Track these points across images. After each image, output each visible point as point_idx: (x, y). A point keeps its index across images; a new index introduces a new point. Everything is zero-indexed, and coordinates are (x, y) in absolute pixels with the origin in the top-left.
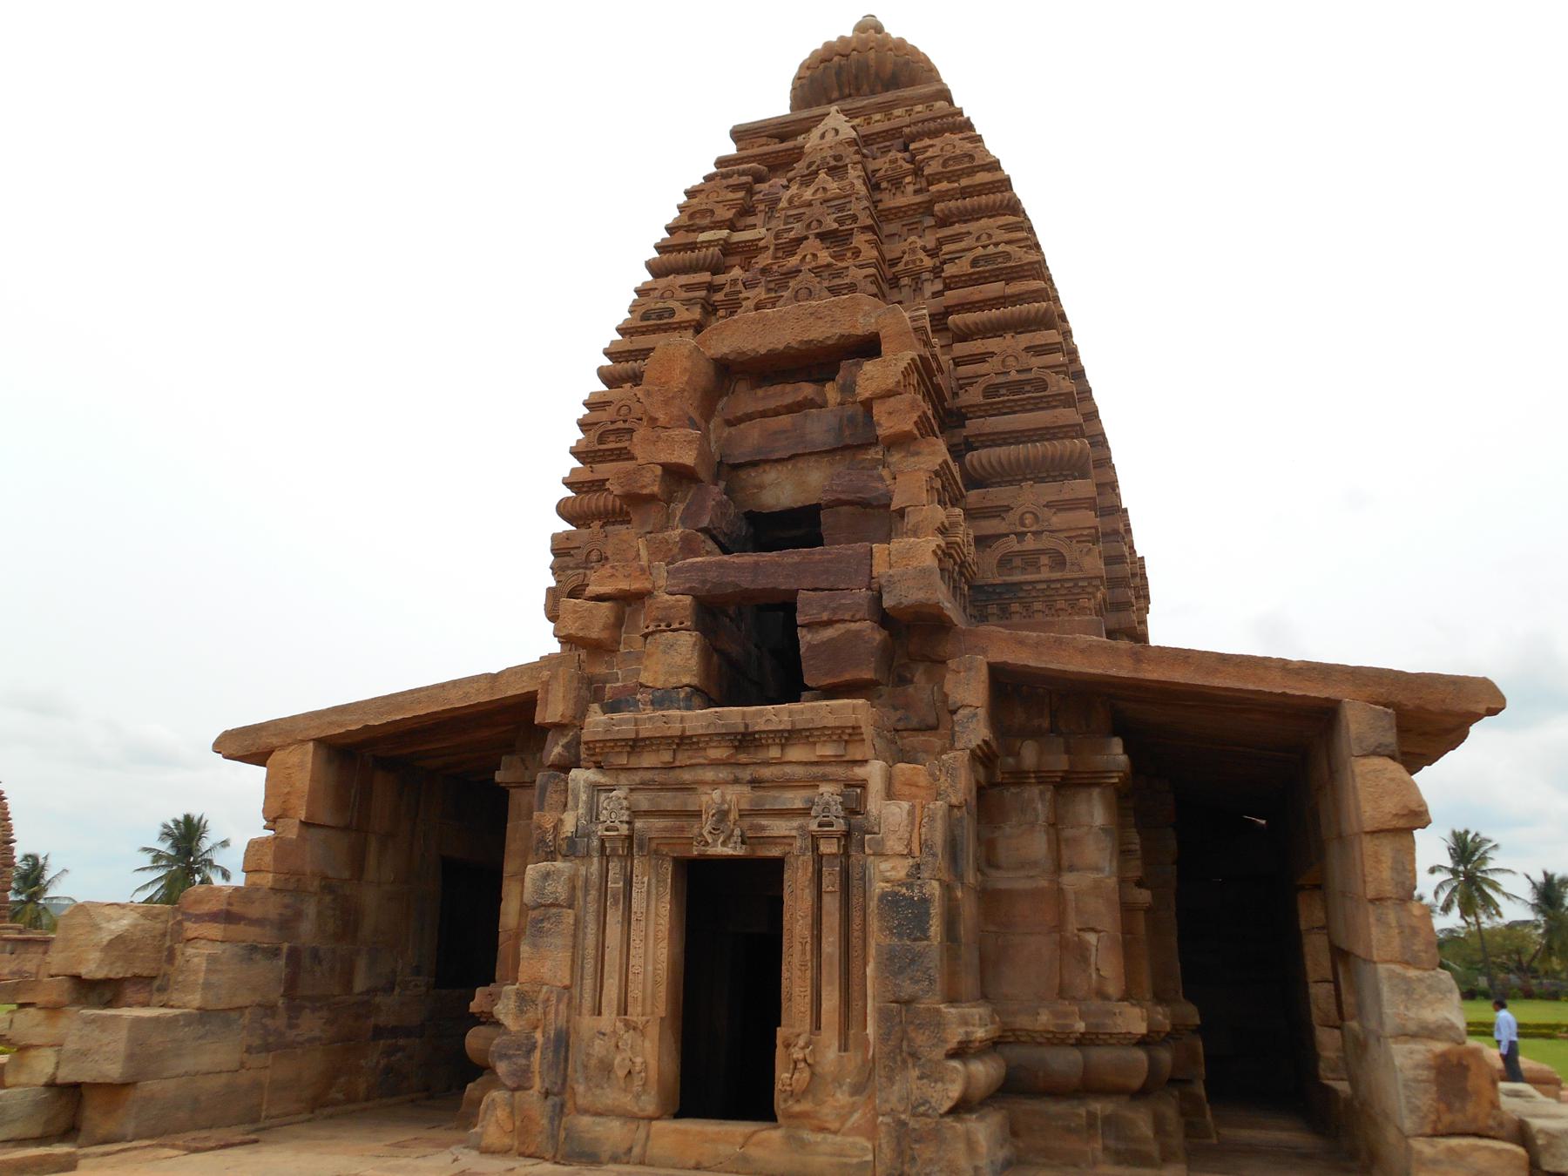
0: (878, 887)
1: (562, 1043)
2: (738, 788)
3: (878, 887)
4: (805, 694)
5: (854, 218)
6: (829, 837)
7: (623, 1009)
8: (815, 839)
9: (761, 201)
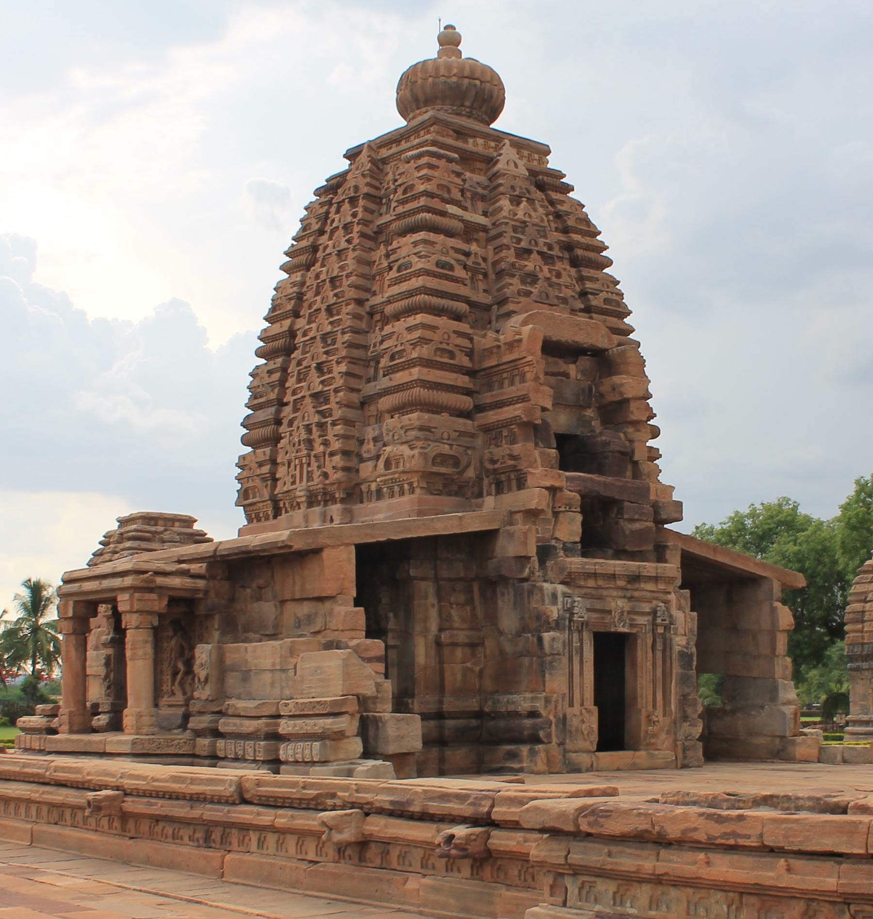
0: (677, 649)
1: (563, 721)
2: (623, 600)
3: (677, 649)
4: (610, 552)
5: (550, 247)
6: (661, 625)
7: (582, 704)
8: (654, 624)
9: (469, 190)
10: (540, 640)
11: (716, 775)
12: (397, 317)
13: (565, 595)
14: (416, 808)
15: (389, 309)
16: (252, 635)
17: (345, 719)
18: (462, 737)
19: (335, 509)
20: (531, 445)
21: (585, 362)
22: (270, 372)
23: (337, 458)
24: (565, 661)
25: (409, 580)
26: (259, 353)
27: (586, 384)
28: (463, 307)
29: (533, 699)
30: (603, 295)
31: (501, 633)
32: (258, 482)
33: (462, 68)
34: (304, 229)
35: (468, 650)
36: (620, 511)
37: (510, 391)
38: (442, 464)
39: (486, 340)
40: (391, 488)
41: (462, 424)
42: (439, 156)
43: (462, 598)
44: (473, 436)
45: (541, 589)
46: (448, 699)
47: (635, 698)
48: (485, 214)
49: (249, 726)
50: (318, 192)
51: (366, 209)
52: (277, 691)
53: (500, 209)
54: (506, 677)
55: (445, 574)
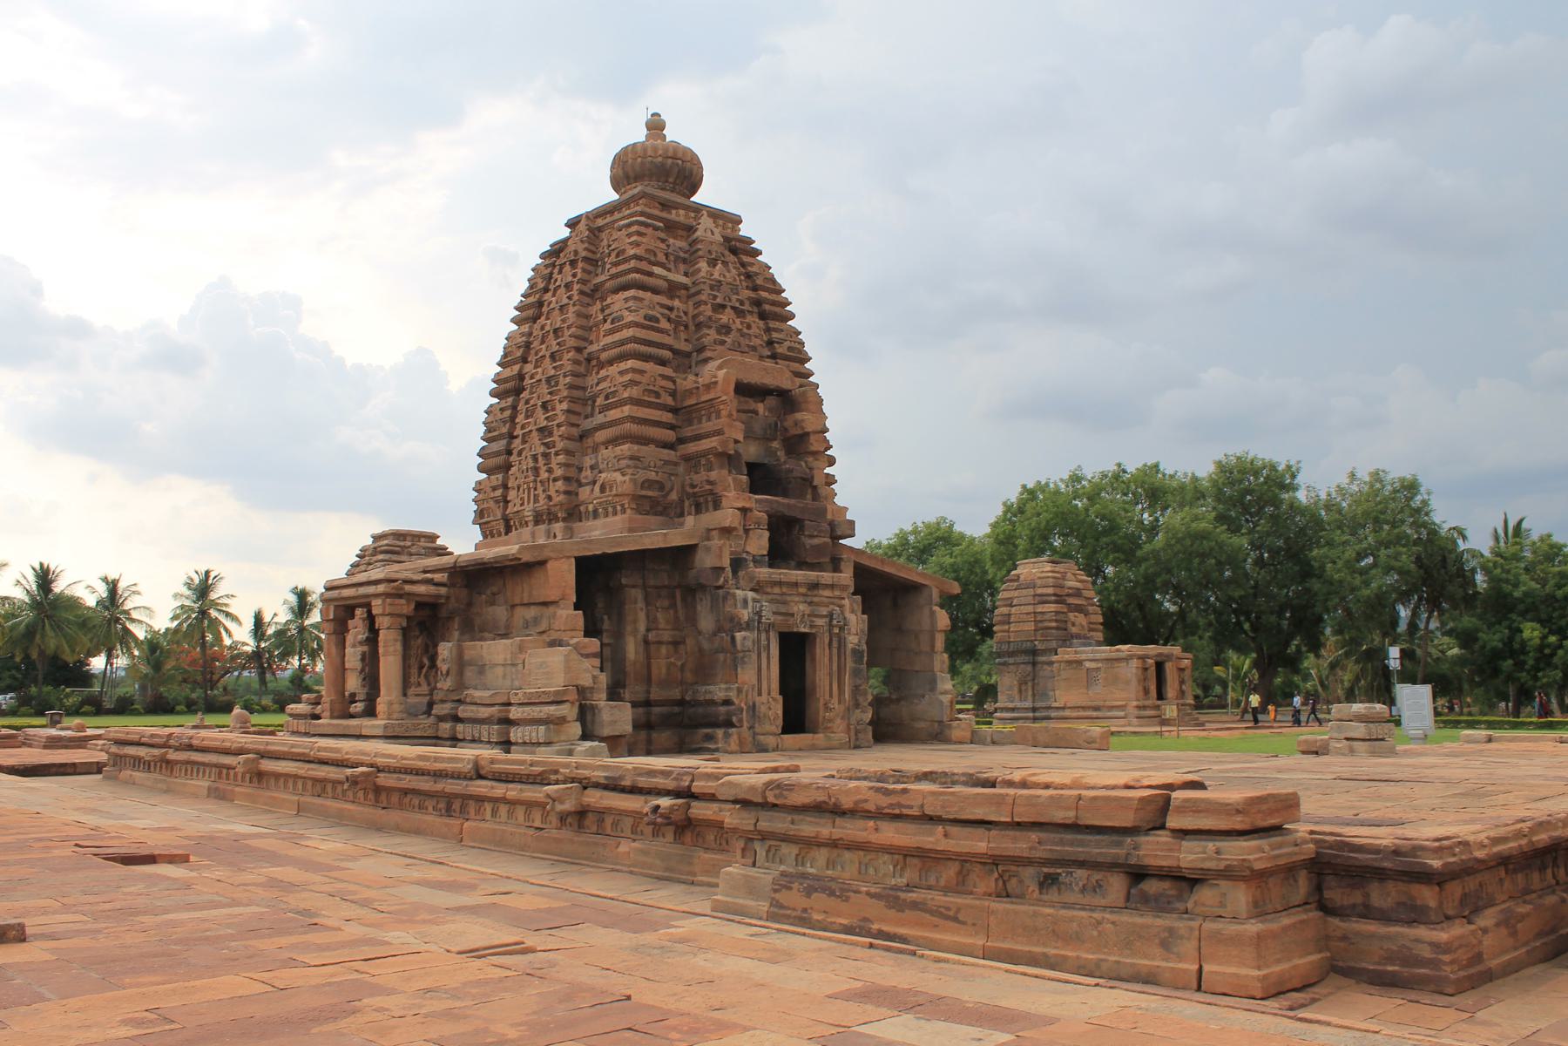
0: (850, 646)
1: (753, 708)
3: (850, 646)
4: (793, 563)
5: (742, 303)
8: (831, 625)
10: (733, 638)
11: (884, 755)
12: (611, 362)
13: (754, 600)
14: (627, 783)
15: (604, 356)
16: (486, 635)
17: (567, 705)
18: (666, 722)
19: (558, 527)
20: (725, 472)
21: (772, 401)
22: (502, 410)
23: (560, 483)
24: (754, 656)
25: (621, 587)
26: (493, 394)
27: (773, 420)
28: (667, 354)
29: (727, 689)
30: (787, 344)
31: (700, 633)
32: (491, 504)
33: (666, 149)
34: (531, 287)
35: (671, 647)
36: (802, 528)
37: (707, 426)
38: (649, 488)
39: (687, 382)
40: (606, 509)
41: (667, 454)
42: (647, 225)
43: (666, 603)
44: (676, 464)
45: (734, 596)
46: (654, 689)
47: (814, 689)
48: (686, 274)
49: (484, 712)
50: (543, 256)
51: (584, 270)
52: (508, 683)
53: (699, 270)
54: (704, 670)
55: (652, 582)
